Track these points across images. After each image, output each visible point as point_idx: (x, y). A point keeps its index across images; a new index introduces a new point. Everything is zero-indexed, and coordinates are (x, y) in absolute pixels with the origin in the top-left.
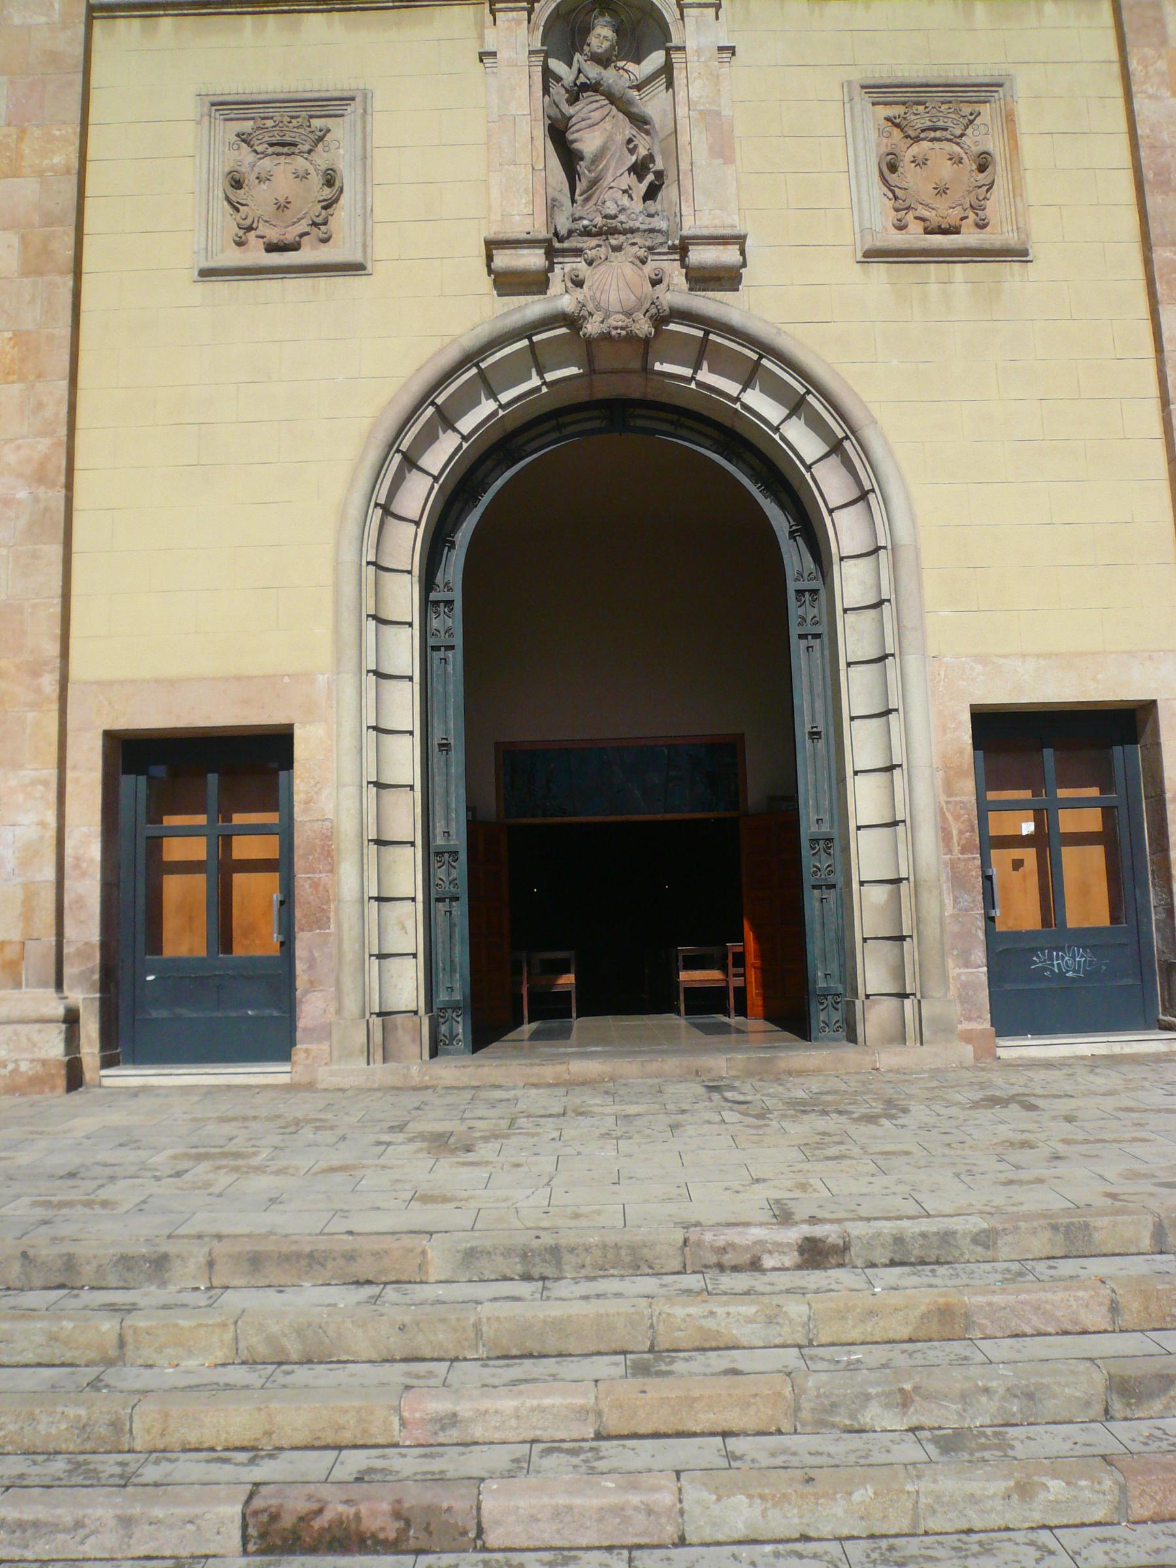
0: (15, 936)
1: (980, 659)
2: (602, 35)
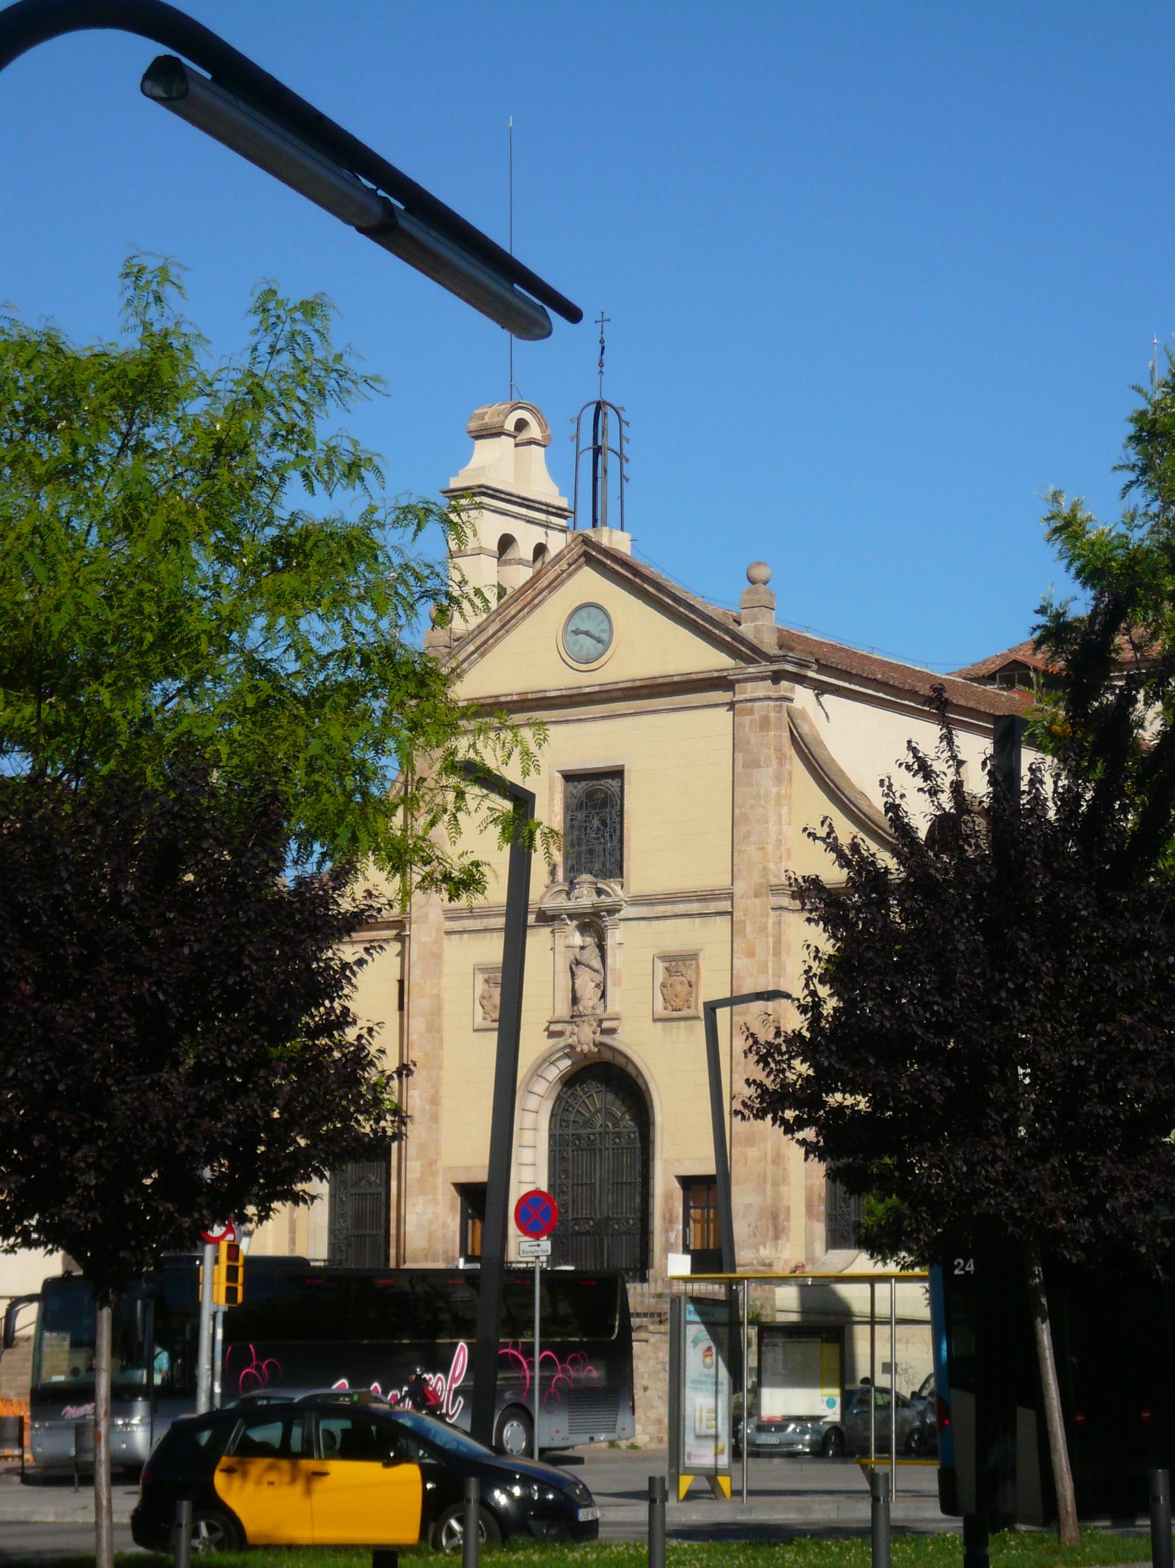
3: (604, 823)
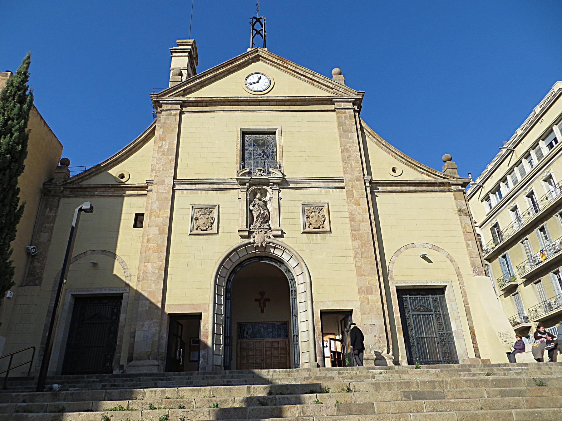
0: (150, 350)
1: (321, 301)
2: (258, 196)
3: (264, 152)
